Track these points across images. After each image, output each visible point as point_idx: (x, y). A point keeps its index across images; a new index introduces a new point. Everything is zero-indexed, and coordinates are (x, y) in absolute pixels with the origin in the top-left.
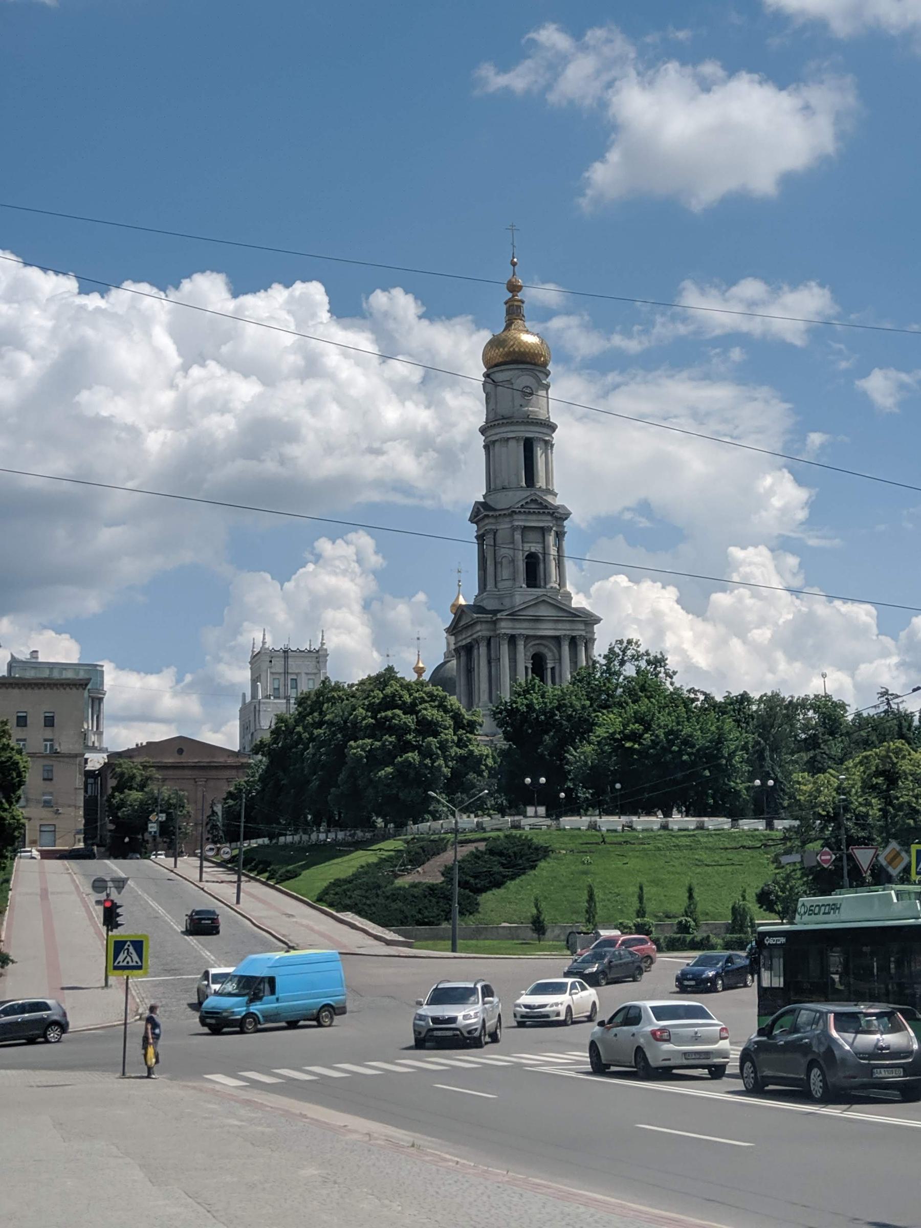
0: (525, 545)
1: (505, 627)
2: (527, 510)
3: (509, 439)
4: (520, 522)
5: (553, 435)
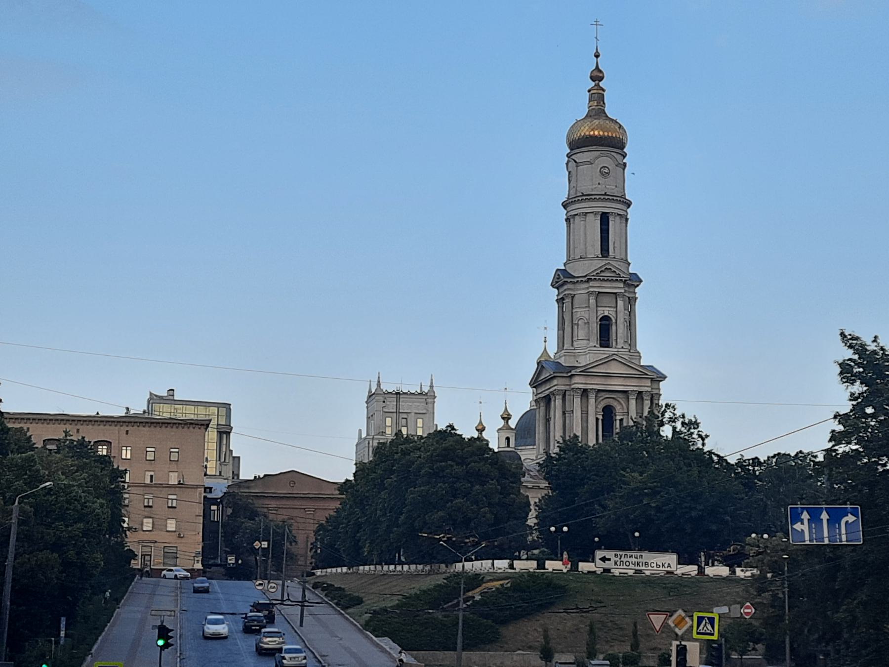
0: (599, 309)
1: (579, 382)
2: (602, 278)
3: (587, 213)
4: (595, 287)
5: (628, 210)
